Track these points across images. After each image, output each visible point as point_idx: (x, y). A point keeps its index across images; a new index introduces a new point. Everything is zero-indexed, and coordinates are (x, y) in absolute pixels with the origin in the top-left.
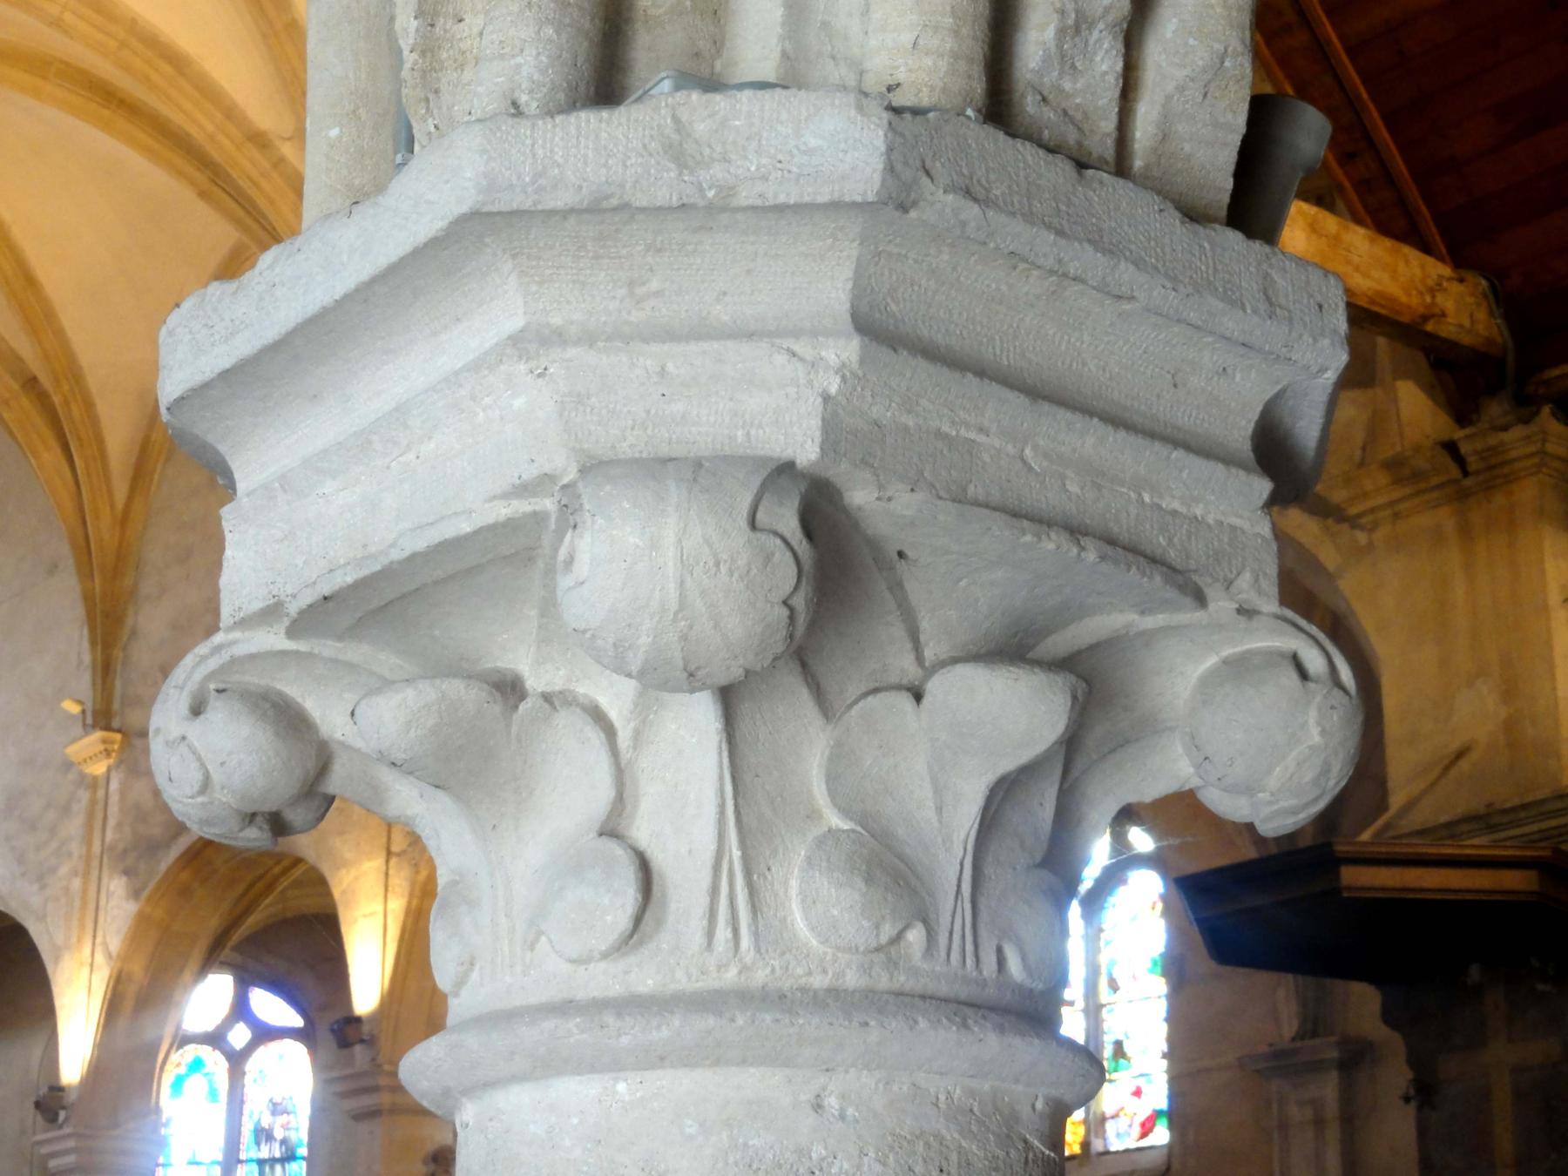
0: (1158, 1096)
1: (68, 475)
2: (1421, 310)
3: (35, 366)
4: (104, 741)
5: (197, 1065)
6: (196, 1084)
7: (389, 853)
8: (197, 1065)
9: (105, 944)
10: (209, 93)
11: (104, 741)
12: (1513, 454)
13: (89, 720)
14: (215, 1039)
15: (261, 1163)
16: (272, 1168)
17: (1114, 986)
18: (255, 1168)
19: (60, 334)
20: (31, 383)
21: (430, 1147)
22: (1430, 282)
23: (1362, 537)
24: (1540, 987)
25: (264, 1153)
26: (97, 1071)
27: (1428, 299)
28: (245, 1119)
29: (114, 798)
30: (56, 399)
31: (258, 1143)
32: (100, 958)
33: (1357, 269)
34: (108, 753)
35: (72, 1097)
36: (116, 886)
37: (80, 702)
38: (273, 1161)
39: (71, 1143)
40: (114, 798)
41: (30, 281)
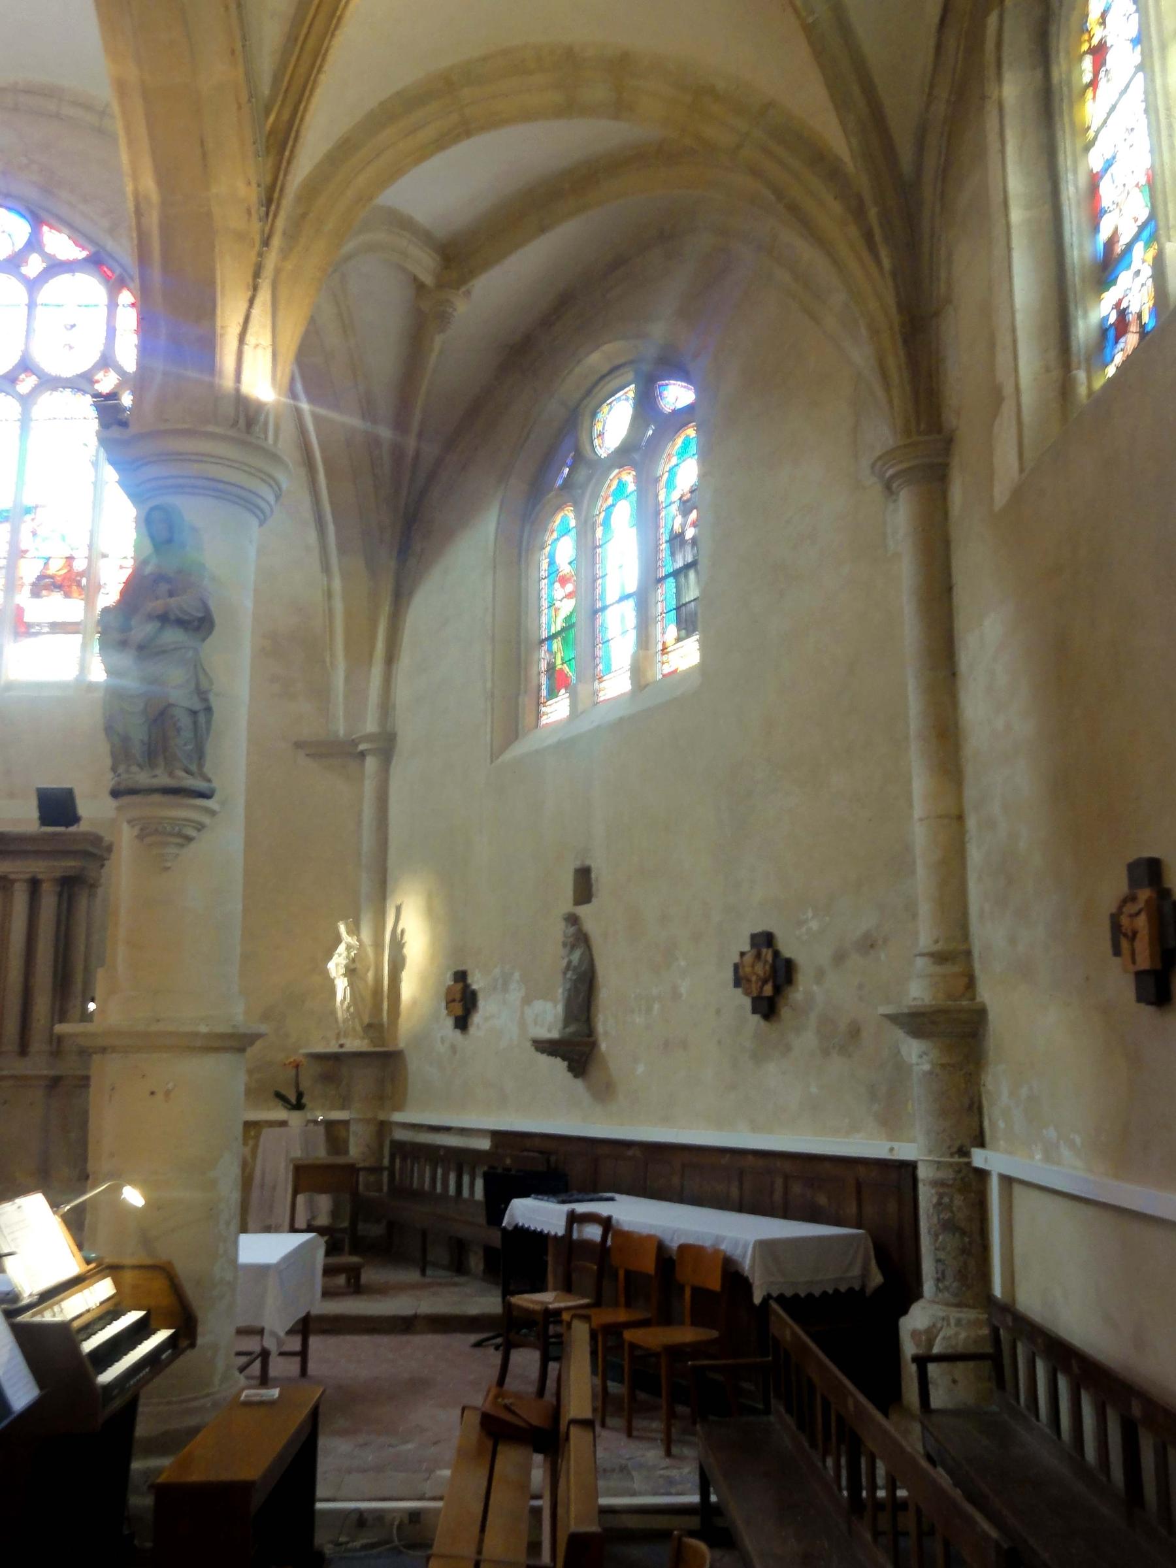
15: (676, 574)
16: (686, 576)
18: (671, 580)
25: (680, 564)
31: (673, 554)
38: (688, 566)
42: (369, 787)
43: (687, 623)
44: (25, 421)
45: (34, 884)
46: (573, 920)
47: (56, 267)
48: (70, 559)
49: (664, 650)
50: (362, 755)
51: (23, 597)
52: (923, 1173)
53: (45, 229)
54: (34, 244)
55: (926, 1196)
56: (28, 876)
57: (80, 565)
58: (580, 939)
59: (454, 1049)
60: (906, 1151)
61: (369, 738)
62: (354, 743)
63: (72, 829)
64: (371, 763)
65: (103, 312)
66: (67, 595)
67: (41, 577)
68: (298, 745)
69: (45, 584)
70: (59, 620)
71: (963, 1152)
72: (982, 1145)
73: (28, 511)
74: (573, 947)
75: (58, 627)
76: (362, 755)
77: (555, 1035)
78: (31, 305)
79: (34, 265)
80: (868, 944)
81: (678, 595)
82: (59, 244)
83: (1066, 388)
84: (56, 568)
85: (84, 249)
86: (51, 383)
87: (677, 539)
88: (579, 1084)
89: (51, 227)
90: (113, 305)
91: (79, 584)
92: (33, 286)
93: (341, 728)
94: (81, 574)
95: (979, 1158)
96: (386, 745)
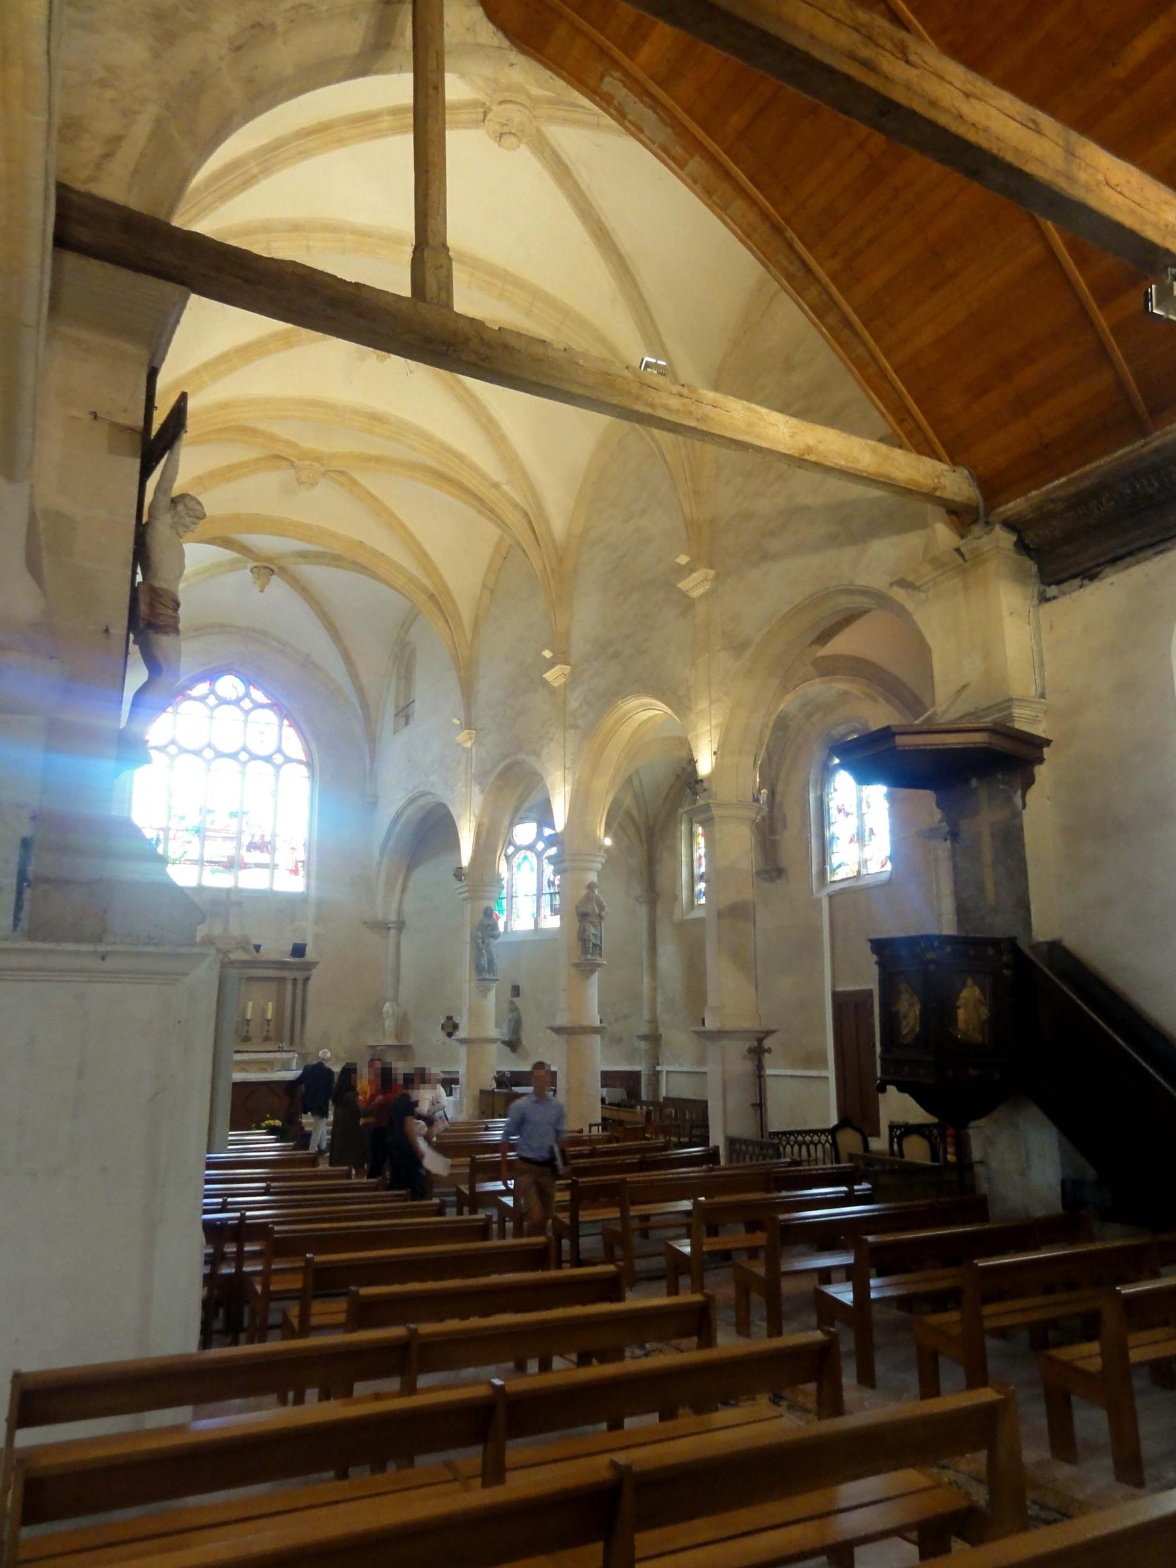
0: (886, 850)
1: (448, 630)
2: (933, 486)
3: (432, 590)
4: (469, 734)
5: (525, 858)
6: (526, 866)
7: (565, 767)
8: (525, 858)
9: (474, 812)
10: (474, 469)
11: (469, 734)
12: (985, 549)
13: (463, 725)
14: (531, 847)
15: (551, 894)
17: (869, 806)
19: (441, 577)
20: (432, 597)
21: (587, 883)
22: (937, 473)
23: (923, 596)
24: (1002, 787)
25: (552, 891)
26: (474, 860)
27: (936, 481)
28: (544, 878)
29: (474, 756)
30: (441, 602)
31: (549, 887)
32: (472, 816)
33: (898, 469)
34: (471, 740)
35: (464, 872)
36: (476, 789)
37: (459, 719)
39: (466, 888)
40: (474, 756)
41: (426, 555)
42: (392, 941)
43: (554, 911)
44: (243, 773)
45: (295, 980)
46: (512, 1003)
47: (258, 706)
48: (263, 836)
49: (545, 917)
50: (389, 928)
51: (243, 851)
52: (643, 1072)
53: (251, 687)
54: (247, 695)
55: (643, 1077)
56: (292, 977)
57: (267, 839)
58: (514, 1008)
59: (444, 1043)
60: (636, 1068)
61: (393, 922)
62: (387, 924)
63: (302, 960)
64: (393, 933)
65: (276, 728)
66: (262, 852)
67: (251, 843)
68: (365, 923)
69: (252, 846)
70: (259, 862)
71: (655, 1068)
72: (658, 1064)
73: (244, 813)
74: (512, 1011)
75: (258, 866)
76: (389, 928)
77: (507, 1039)
78: (246, 722)
79: (247, 704)
80: (626, 1017)
81: (551, 901)
82: (258, 695)
83: (692, 902)
84: (257, 839)
85: (269, 699)
86: (254, 757)
87: (551, 883)
88: (512, 1055)
89: (255, 687)
90: (281, 726)
91: (267, 848)
92: (247, 713)
93: (380, 917)
94: (269, 843)
95: (658, 1068)
96: (400, 926)
